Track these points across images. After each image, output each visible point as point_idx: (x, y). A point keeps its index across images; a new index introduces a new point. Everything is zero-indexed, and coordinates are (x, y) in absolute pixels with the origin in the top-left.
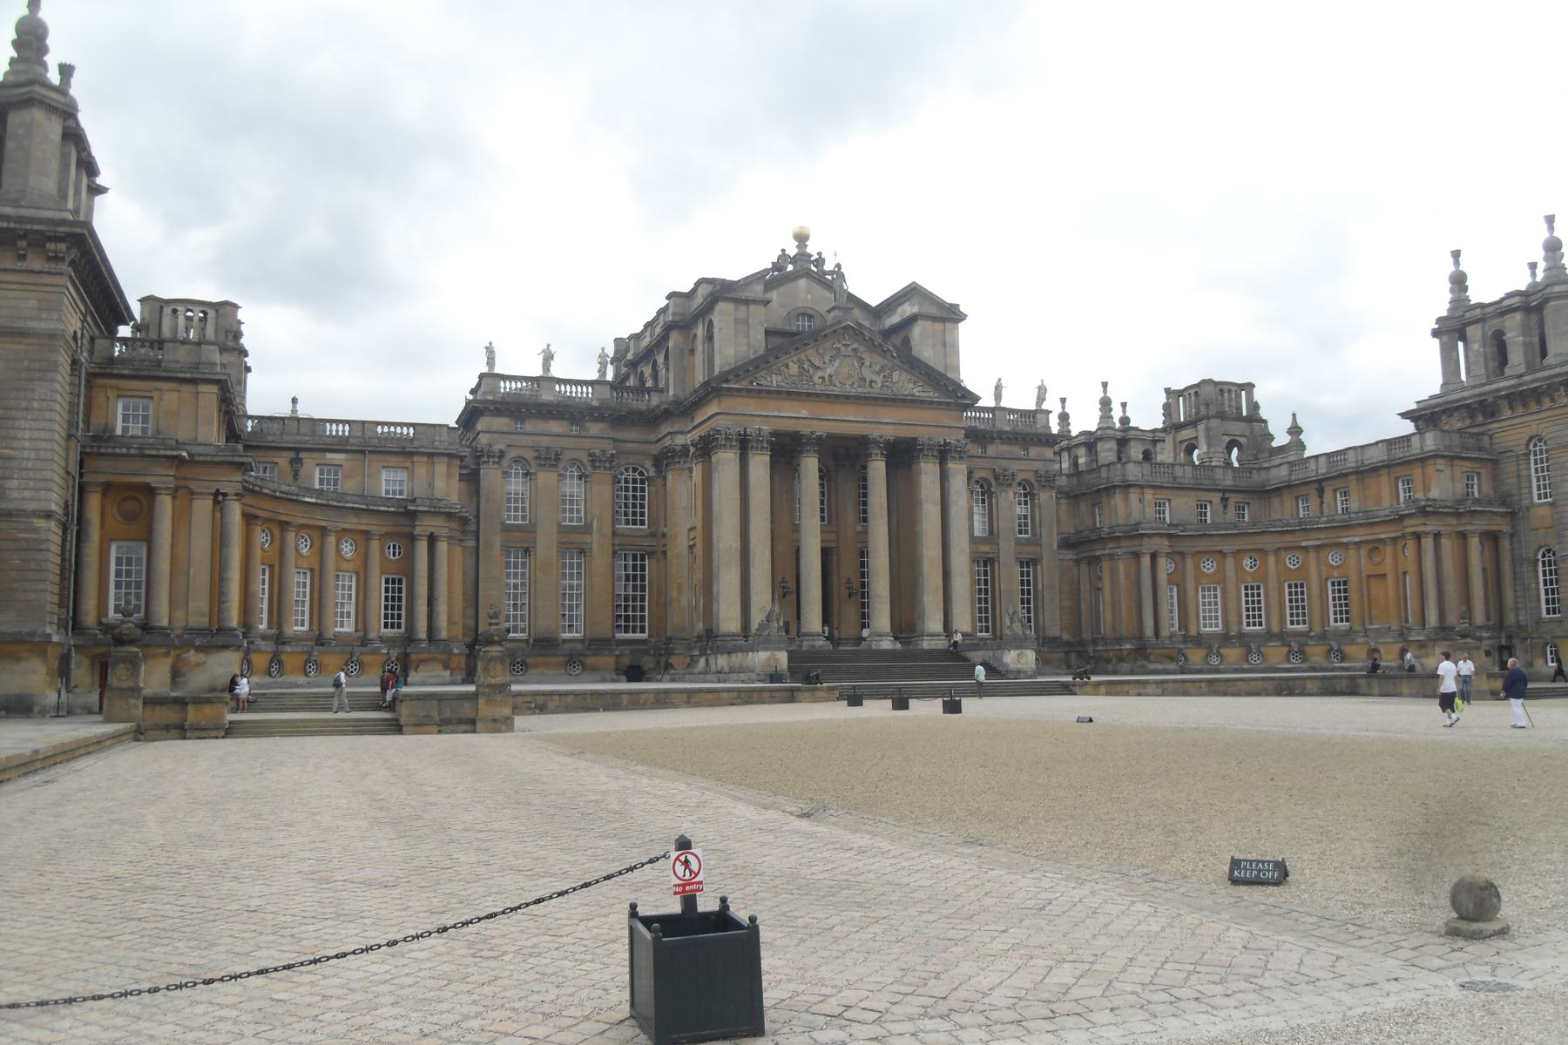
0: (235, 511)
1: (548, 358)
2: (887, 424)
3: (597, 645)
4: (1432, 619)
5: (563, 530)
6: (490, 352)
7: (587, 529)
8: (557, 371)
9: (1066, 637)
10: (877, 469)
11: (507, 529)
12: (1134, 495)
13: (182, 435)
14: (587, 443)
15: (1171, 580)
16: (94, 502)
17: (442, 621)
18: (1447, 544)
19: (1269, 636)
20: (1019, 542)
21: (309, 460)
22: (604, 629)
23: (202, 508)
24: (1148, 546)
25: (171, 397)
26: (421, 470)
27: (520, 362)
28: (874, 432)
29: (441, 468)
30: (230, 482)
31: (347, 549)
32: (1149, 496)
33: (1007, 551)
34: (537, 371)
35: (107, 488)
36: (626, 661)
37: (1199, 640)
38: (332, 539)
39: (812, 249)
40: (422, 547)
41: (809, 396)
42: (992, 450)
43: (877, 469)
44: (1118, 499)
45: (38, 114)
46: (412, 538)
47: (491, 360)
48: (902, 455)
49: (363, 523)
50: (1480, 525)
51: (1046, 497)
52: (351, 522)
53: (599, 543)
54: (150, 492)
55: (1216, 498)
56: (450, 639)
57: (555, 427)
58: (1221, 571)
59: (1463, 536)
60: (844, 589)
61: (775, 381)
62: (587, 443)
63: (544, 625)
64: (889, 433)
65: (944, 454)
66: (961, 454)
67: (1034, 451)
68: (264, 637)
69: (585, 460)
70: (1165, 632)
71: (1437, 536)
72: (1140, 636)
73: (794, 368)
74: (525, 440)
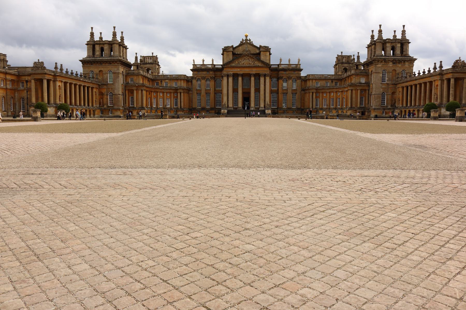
0: (144, 92)
1: (203, 61)
2: (254, 71)
3: (212, 109)
4: (349, 106)
5: (206, 90)
6: (194, 60)
7: (210, 90)
8: (205, 63)
9: (302, 108)
10: (253, 79)
11: (197, 90)
12: (311, 81)
13: (137, 82)
14: (210, 75)
15: (316, 97)
16: (127, 92)
17: (182, 105)
18: (354, 92)
19: (334, 108)
20: (292, 90)
21: (163, 81)
22: (213, 106)
23: (140, 92)
24: (311, 91)
25: (135, 78)
26: (179, 82)
27: (199, 62)
28: (251, 72)
29: (182, 82)
30: (143, 88)
31: (168, 95)
32: (314, 81)
33: (290, 91)
34: (202, 63)
35: (128, 90)
36: (217, 111)
37: (322, 109)
38: (165, 93)
39: (248, 39)
40: (179, 94)
41: (239, 67)
42: (287, 73)
43: (253, 79)
44: (308, 82)
45: (115, 45)
46: (177, 93)
47: (194, 62)
48: (258, 76)
49: (171, 91)
50: (361, 88)
51: (299, 81)
52: (168, 91)
53: (212, 91)
54: (133, 90)
55: (330, 81)
56: (184, 108)
57: (204, 73)
58: (327, 95)
59: (358, 90)
60: (246, 99)
61: (233, 65)
62: (210, 75)
63: (203, 105)
64: (254, 72)
65: (265, 76)
66: (268, 76)
67: (296, 72)
68: (154, 108)
69: (210, 78)
70: (314, 107)
71: (352, 90)
72: (309, 108)
73: (237, 62)
74: (200, 75)
